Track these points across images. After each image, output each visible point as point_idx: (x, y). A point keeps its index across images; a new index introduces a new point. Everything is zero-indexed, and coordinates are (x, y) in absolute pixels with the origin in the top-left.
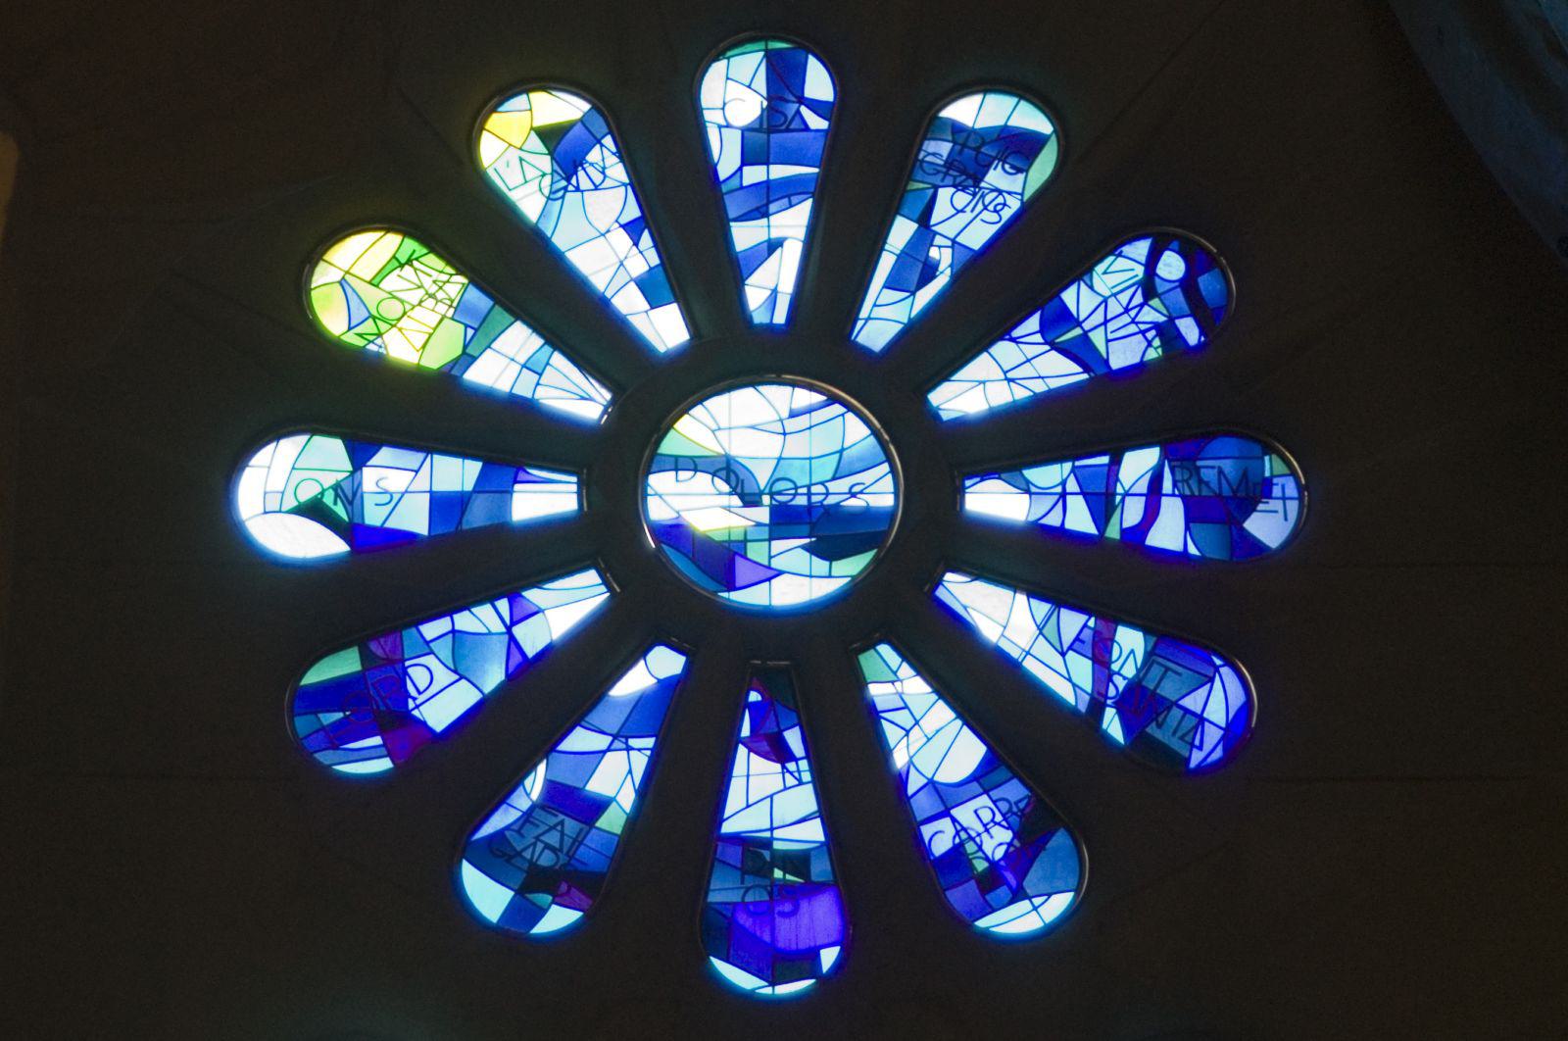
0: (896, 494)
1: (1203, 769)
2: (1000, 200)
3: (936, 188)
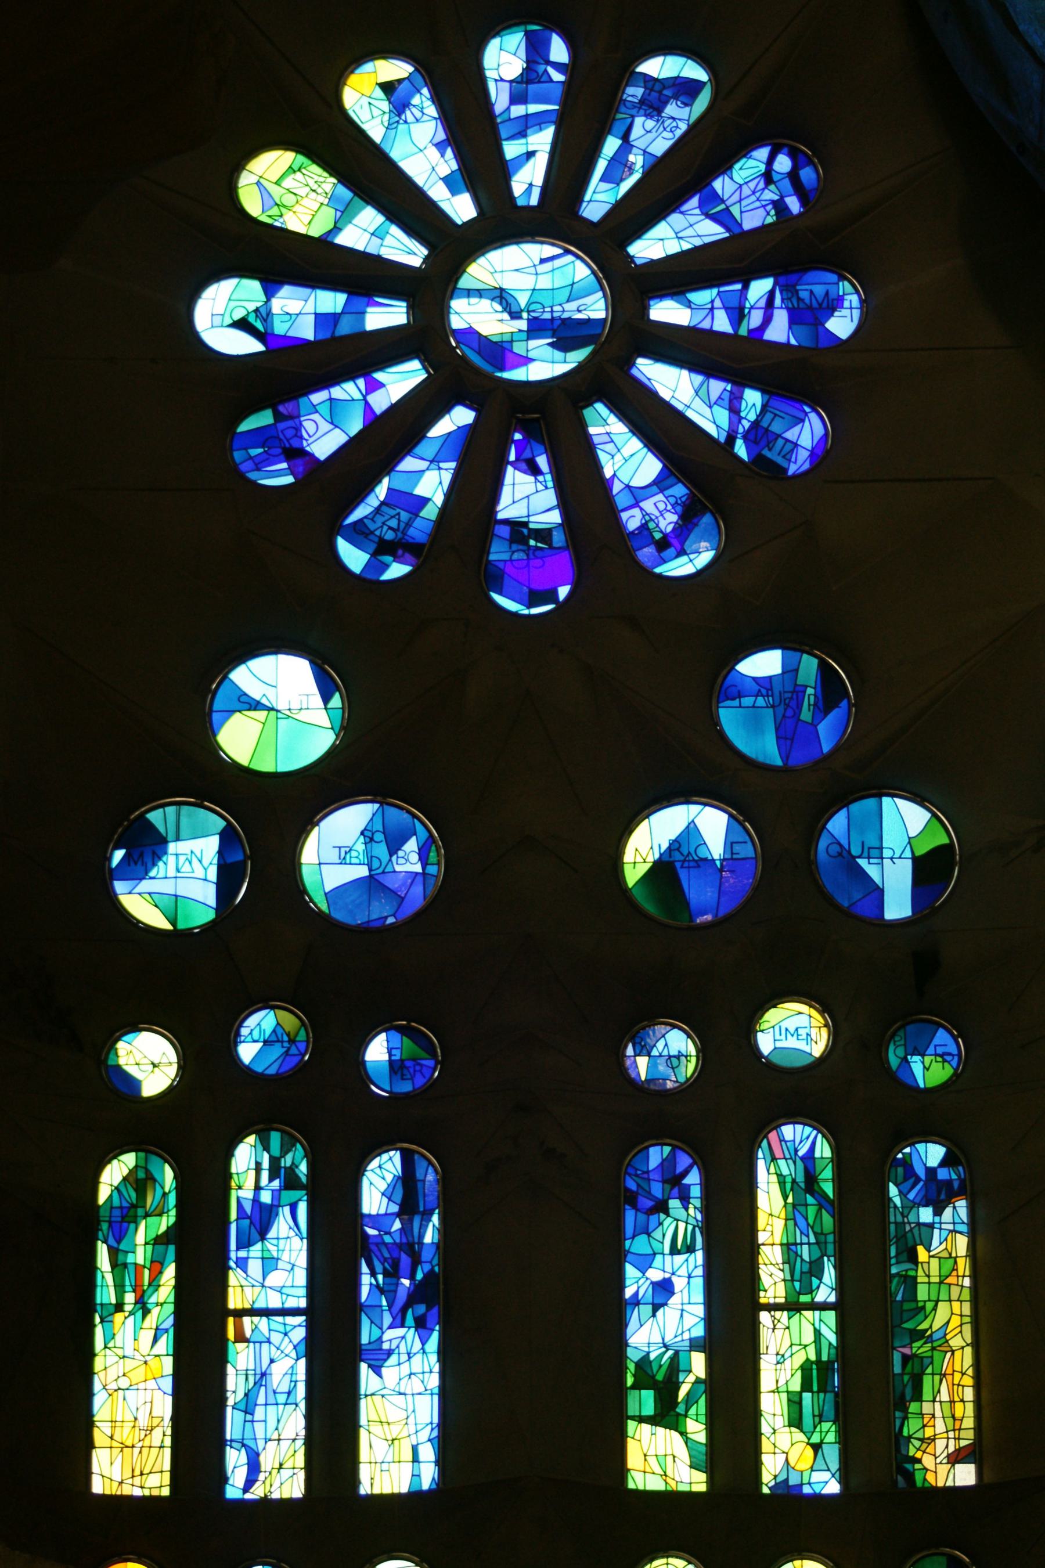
0: (607, 309)
1: (795, 476)
2: (674, 124)
3: (633, 117)
